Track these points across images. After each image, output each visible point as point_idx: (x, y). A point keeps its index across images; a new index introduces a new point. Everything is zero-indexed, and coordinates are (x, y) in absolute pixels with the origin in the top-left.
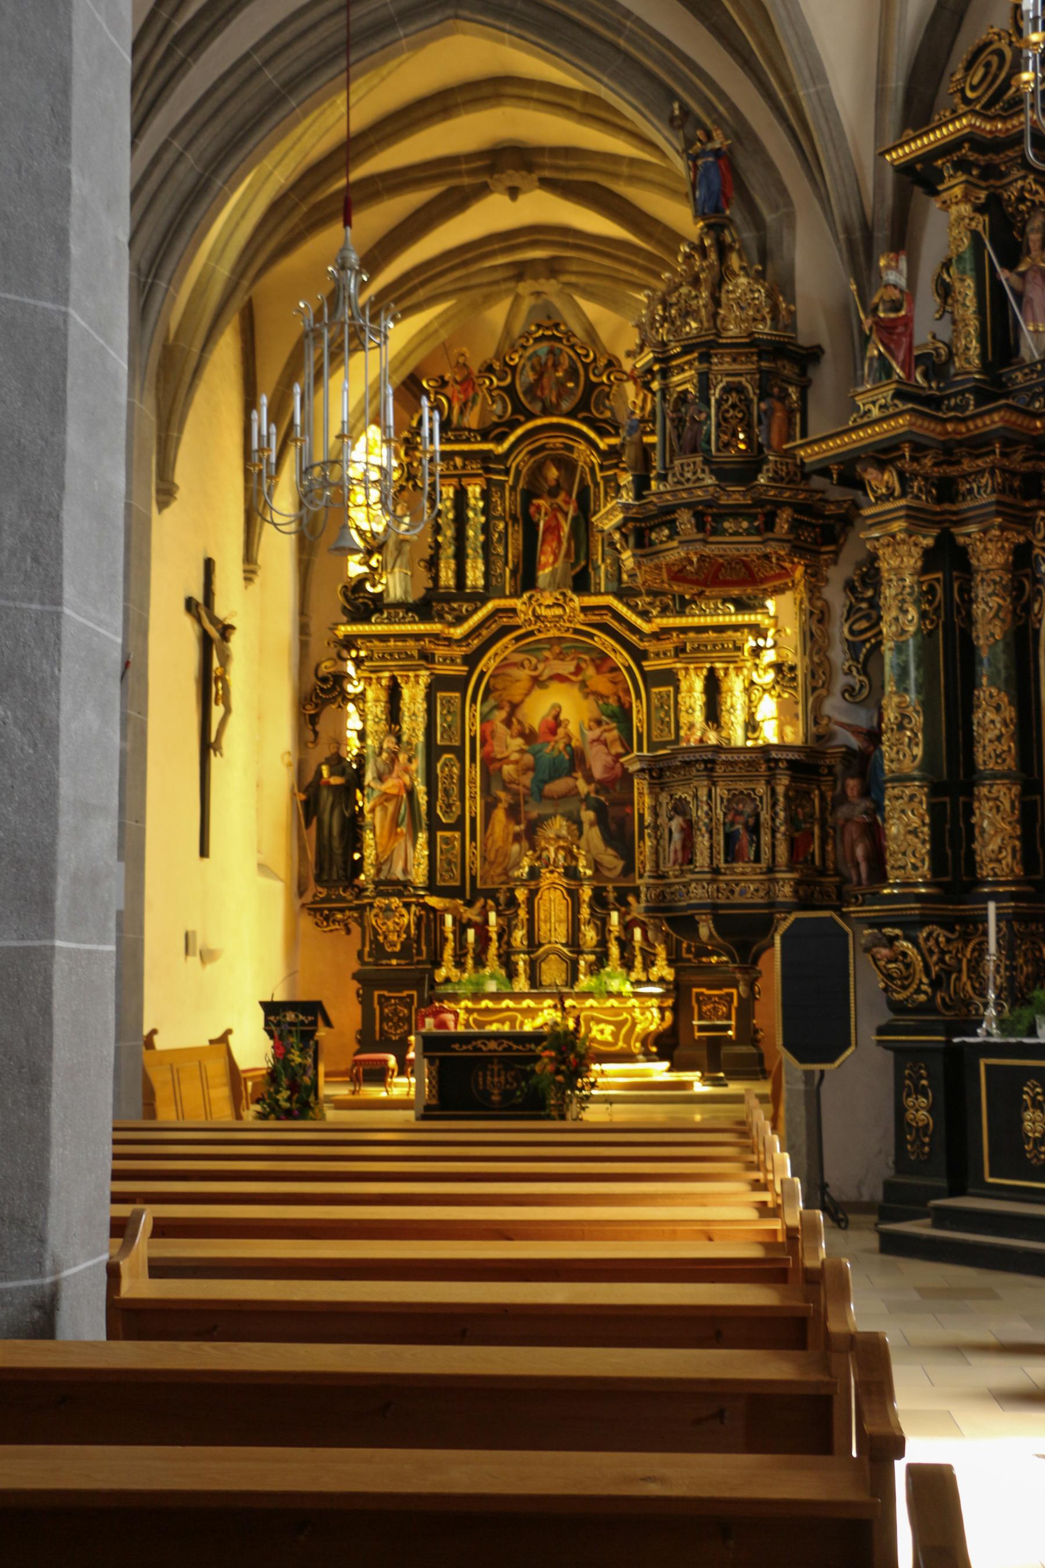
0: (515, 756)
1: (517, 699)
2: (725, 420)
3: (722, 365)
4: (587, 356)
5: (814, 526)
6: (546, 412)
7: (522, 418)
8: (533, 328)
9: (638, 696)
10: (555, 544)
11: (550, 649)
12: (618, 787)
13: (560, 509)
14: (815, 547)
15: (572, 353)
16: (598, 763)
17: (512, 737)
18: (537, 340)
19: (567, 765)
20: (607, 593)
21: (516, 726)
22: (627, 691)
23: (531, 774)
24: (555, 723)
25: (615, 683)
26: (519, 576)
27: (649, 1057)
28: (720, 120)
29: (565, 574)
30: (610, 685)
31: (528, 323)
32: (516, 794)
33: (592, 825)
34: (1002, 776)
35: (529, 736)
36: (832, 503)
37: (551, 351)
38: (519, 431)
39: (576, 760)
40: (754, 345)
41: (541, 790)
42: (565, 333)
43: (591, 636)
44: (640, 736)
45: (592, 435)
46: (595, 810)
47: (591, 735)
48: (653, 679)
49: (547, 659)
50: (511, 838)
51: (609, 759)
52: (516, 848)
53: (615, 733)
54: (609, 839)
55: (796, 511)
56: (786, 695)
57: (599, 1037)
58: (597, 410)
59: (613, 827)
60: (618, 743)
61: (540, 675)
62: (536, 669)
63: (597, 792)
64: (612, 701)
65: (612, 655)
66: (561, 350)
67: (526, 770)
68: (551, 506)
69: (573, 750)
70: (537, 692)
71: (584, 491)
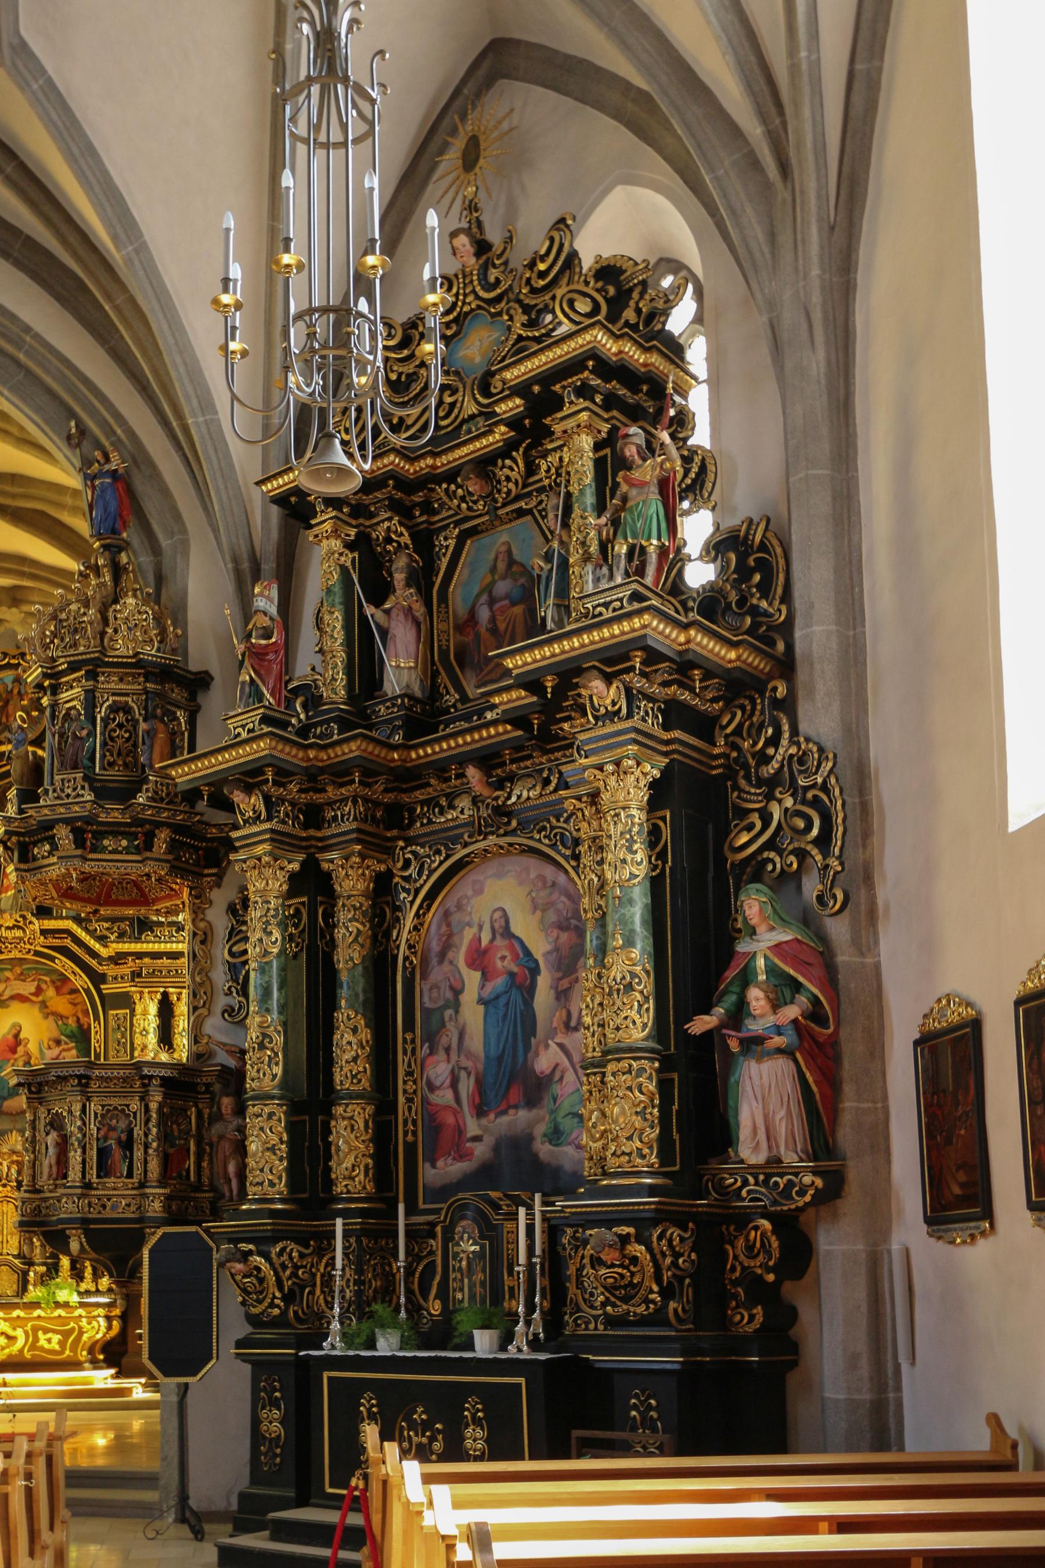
2: (112, 739)
3: (109, 684)
5: (196, 849)
14: (196, 869)
27: (95, 1364)
28: (118, 444)
34: (359, 1096)
36: (214, 826)
40: (138, 665)
55: (175, 832)
57: (46, 1346)
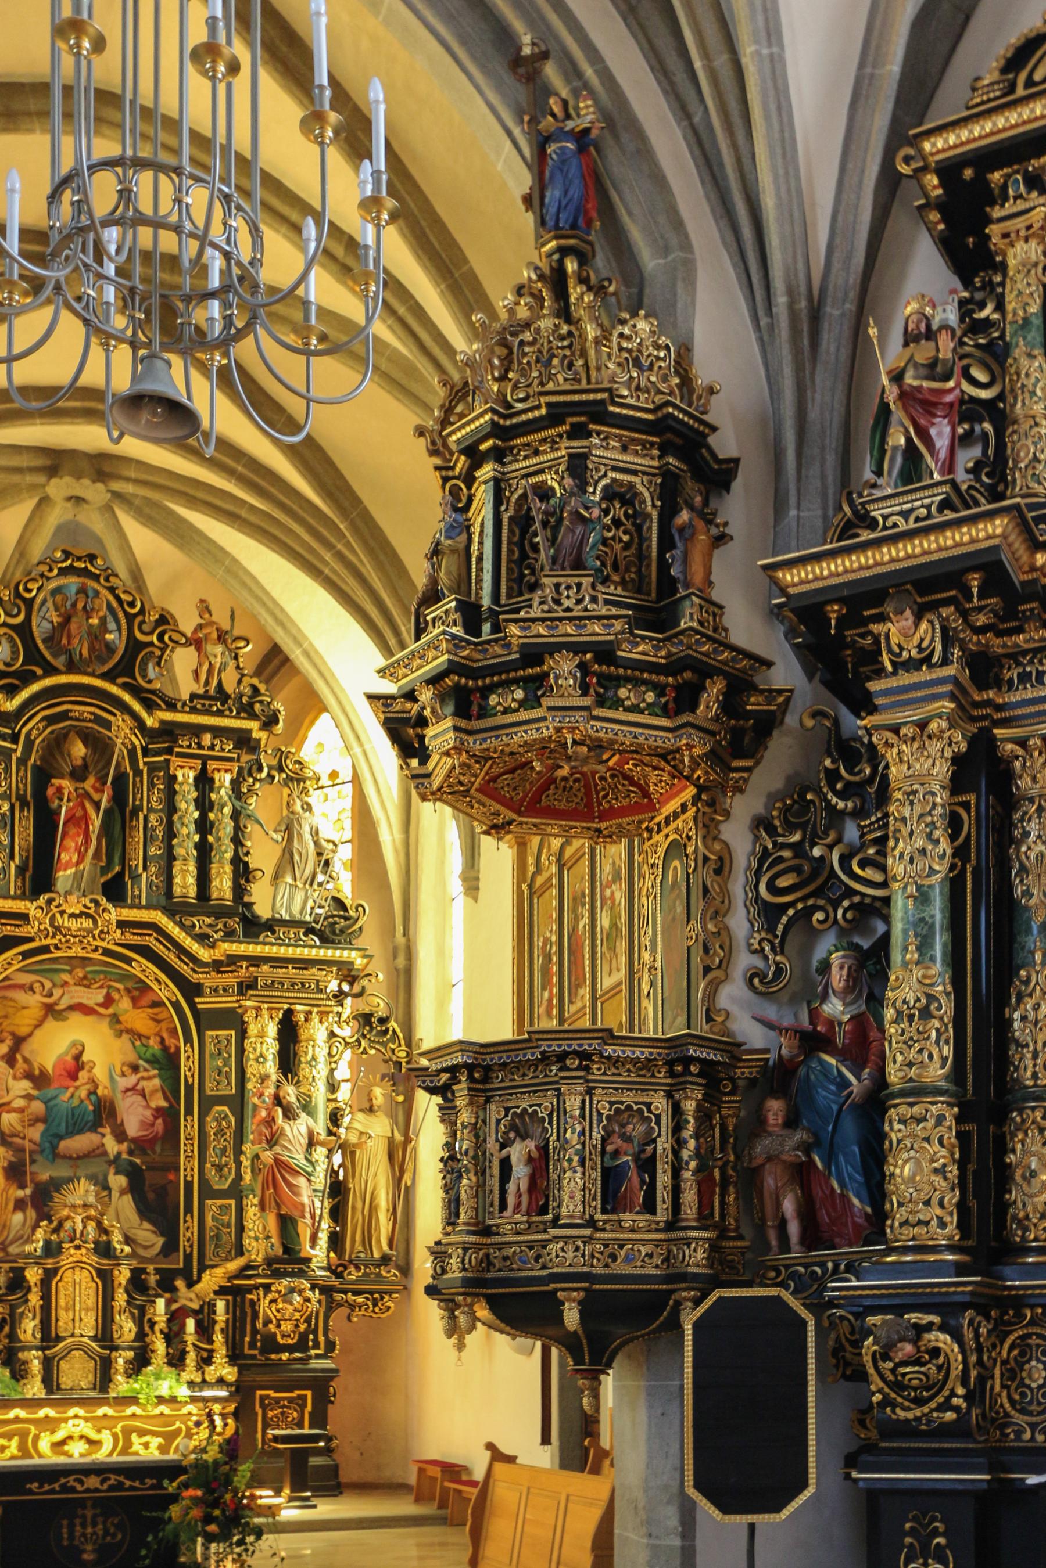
0: (19, 1103)
1: (23, 1031)
4: (132, 604)
6: (72, 667)
7: (39, 672)
8: (59, 554)
9: (188, 1039)
10: (80, 840)
11: (70, 972)
12: (158, 1149)
13: (87, 795)
15: (111, 598)
16: (134, 1117)
17: (15, 1078)
18: (63, 572)
19: (91, 1117)
20: (148, 907)
21: (20, 1063)
22: (174, 1032)
23: (41, 1127)
24: (76, 1065)
25: (158, 1021)
26: (28, 875)
29: (93, 880)
30: (152, 1024)
31: (52, 547)
32: (22, 1150)
33: (122, 1193)
35: (39, 1079)
37: (82, 590)
38: (35, 687)
39: (103, 1113)
41: (54, 1147)
42: (105, 570)
43: (129, 961)
44: (189, 1088)
45: (137, 707)
46: (128, 1175)
47: (124, 1083)
48: (206, 1020)
49: (65, 984)
50: (11, 1206)
51: (148, 1113)
52: (18, 1217)
53: (157, 1082)
54: (145, 1210)
56: (373, 1052)
58: (144, 676)
59: (151, 1196)
60: (160, 1094)
61: (56, 1004)
62: (50, 995)
63: (131, 1153)
64: (154, 1043)
65: (156, 987)
66: (97, 593)
67: (35, 1121)
68: (76, 790)
69: (99, 1100)
70: (51, 1024)
71: (120, 780)
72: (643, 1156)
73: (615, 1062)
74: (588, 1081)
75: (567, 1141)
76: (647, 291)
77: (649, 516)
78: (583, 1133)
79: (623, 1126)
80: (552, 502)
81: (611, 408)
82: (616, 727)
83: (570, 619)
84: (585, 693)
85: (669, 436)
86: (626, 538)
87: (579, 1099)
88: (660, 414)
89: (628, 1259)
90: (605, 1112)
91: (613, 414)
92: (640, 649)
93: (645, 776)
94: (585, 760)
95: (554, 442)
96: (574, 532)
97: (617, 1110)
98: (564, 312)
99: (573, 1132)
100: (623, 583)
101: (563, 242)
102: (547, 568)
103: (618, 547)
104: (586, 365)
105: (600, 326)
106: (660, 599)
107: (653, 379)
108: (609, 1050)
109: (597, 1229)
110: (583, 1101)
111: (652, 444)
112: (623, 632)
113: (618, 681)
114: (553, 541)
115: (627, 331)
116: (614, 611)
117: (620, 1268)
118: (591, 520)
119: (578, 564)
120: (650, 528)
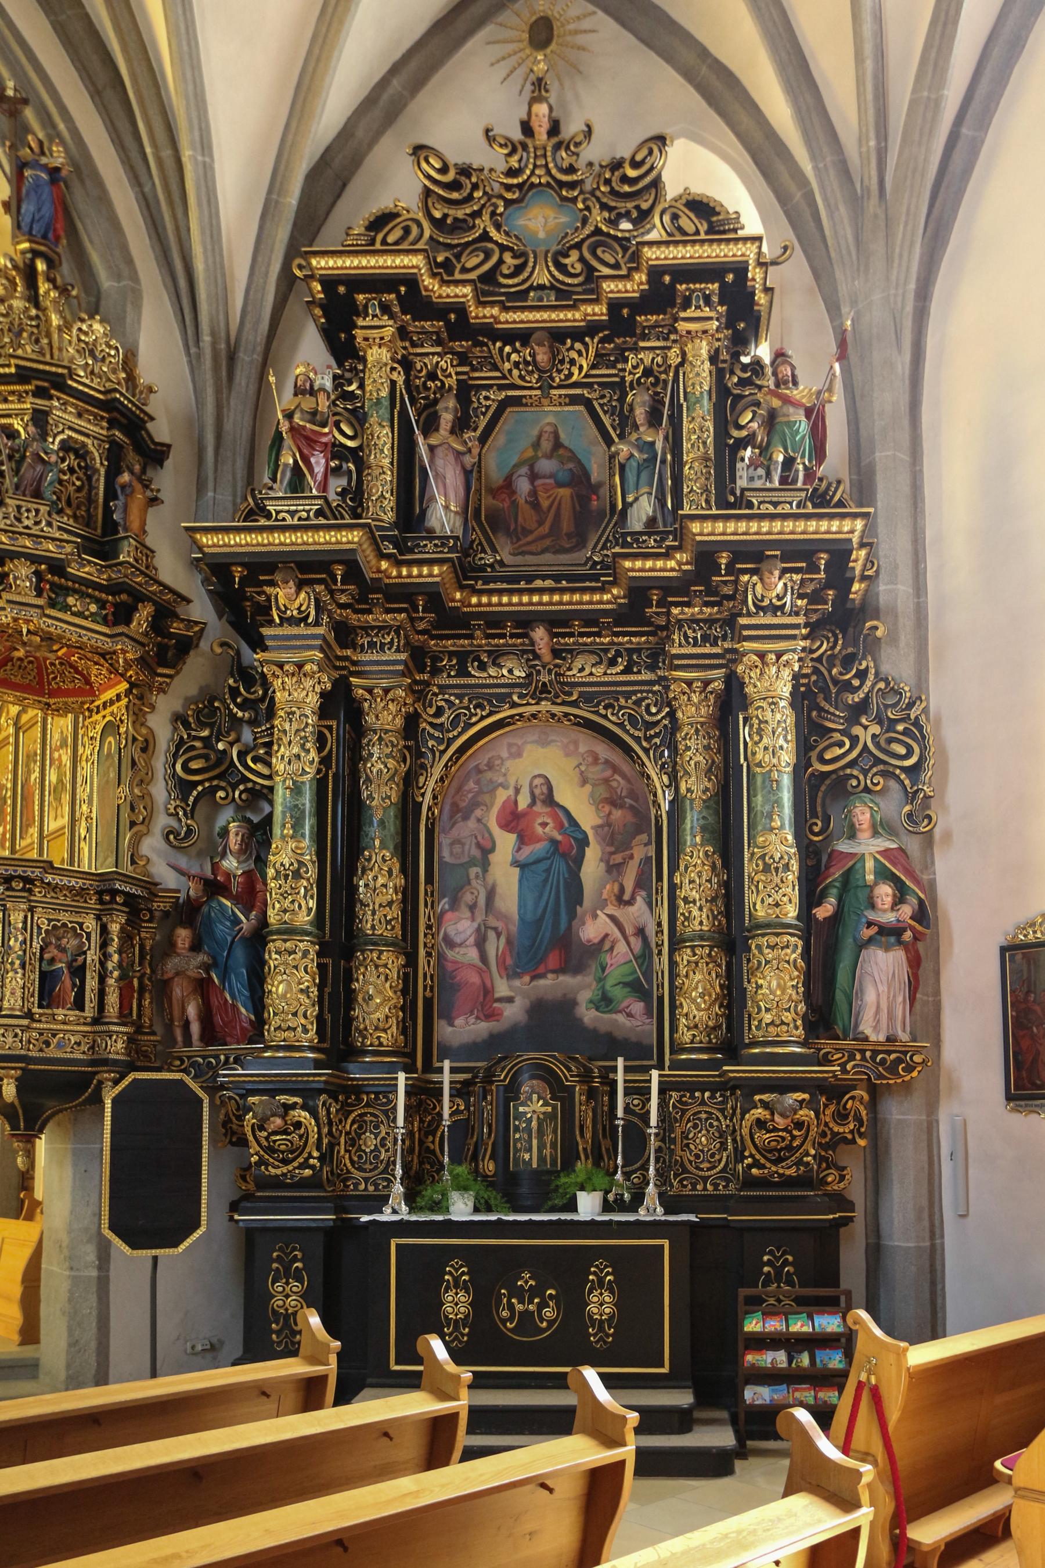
72: (75, 964)
73: (55, 888)
74: (30, 901)
75: (10, 947)
76: (103, 303)
77: (97, 471)
78: (24, 942)
79: (59, 939)
80: (17, 441)
81: (70, 382)
82: (65, 626)
83: (29, 535)
84: (39, 595)
85: (115, 414)
86: (78, 483)
87: (22, 914)
88: (109, 397)
89: (59, 1046)
90: (44, 927)
91: (70, 387)
92: (86, 569)
93: (88, 668)
94: (38, 647)
95: (21, 396)
96: (34, 469)
97: (55, 927)
98: (34, 299)
99: (16, 940)
100: (75, 517)
101: (34, 246)
102: (11, 491)
103: (72, 489)
104: (50, 344)
105: (64, 318)
106: (104, 535)
107: (105, 369)
108: (49, 878)
109: (34, 1020)
110: (26, 917)
111: (102, 418)
112: (72, 554)
113: (67, 591)
114: (17, 472)
115: (84, 327)
116: (65, 536)
117: (52, 1052)
118: (49, 463)
119: (37, 494)
120: (98, 480)
